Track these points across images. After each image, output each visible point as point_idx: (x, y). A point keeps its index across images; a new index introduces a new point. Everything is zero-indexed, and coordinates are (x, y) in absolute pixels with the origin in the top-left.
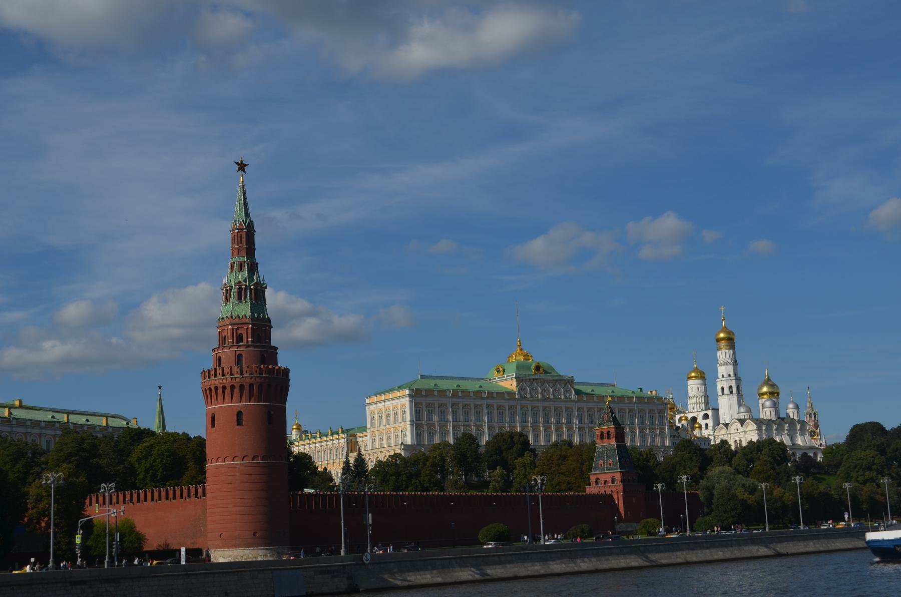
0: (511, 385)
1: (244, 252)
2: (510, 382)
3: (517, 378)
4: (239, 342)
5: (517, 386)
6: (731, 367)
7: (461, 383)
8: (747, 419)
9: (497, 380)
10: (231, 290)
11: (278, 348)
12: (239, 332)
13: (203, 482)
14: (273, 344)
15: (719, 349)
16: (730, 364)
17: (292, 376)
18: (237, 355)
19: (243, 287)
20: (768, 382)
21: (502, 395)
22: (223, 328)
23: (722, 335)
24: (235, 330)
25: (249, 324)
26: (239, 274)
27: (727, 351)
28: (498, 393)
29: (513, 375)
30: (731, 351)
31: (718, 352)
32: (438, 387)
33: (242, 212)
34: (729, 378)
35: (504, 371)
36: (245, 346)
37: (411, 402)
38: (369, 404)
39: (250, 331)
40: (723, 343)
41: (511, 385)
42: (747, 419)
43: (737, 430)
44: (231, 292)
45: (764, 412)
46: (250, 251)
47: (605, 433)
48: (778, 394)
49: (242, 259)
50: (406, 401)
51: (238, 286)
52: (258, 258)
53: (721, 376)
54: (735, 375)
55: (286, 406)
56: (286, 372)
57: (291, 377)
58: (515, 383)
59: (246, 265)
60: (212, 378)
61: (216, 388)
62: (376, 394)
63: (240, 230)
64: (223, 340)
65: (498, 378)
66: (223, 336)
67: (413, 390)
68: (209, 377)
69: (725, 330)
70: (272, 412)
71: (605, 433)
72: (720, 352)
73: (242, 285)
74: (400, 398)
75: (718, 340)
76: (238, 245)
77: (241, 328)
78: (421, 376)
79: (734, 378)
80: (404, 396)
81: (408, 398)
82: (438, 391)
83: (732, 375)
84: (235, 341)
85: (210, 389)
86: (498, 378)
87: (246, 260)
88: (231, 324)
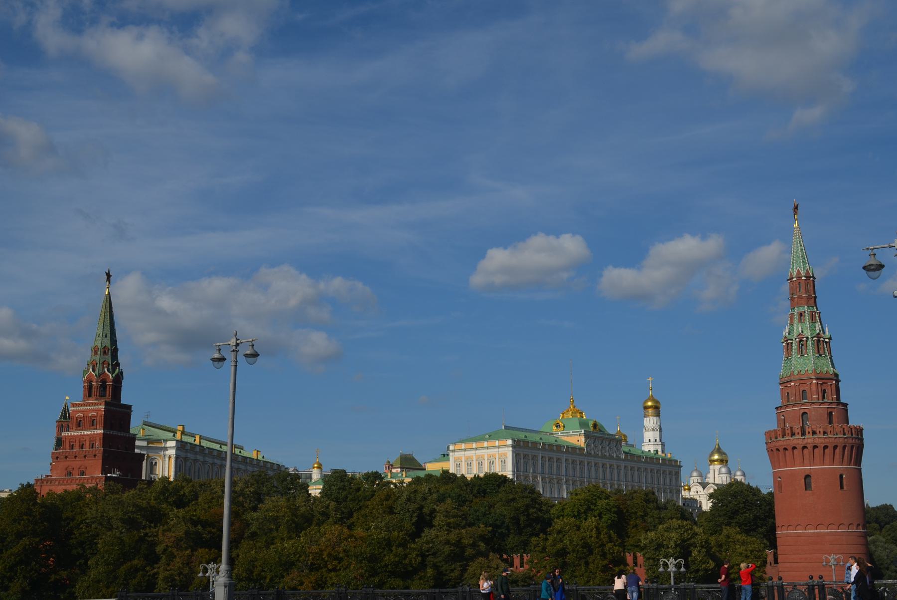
0: (578, 441)
2: (578, 438)
3: (585, 434)
4: (803, 399)
5: (585, 443)
6: (658, 433)
7: (527, 434)
8: (710, 483)
12: (824, 388)
15: (645, 416)
16: (657, 430)
20: (719, 451)
21: (573, 450)
23: (650, 404)
24: (819, 385)
25: (833, 379)
27: (655, 418)
28: (572, 448)
29: (581, 431)
30: (658, 418)
32: (557, 443)
34: (656, 443)
35: (564, 427)
36: (836, 404)
37: (513, 452)
38: (454, 451)
40: (650, 411)
41: (578, 441)
42: (710, 483)
43: (697, 492)
48: (727, 461)
50: (509, 452)
51: (798, 338)
53: (648, 441)
54: (660, 441)
58: (583, 439)
62: (462, 441)
65: (561, 433)
67: (515, 441)
69: (652, 399)
72: (648, 418)
73: (821, 337)
74: (499, 448)
75: (646, 408)
77: (825, 383)
78: (505, 426)
79: (660, 443)
80: (506, 446)
81: (510, 449)
82: (556, 446)
83: (658, 440)
86: (561, 433)
87: (806, 309)
88: (817, 379)
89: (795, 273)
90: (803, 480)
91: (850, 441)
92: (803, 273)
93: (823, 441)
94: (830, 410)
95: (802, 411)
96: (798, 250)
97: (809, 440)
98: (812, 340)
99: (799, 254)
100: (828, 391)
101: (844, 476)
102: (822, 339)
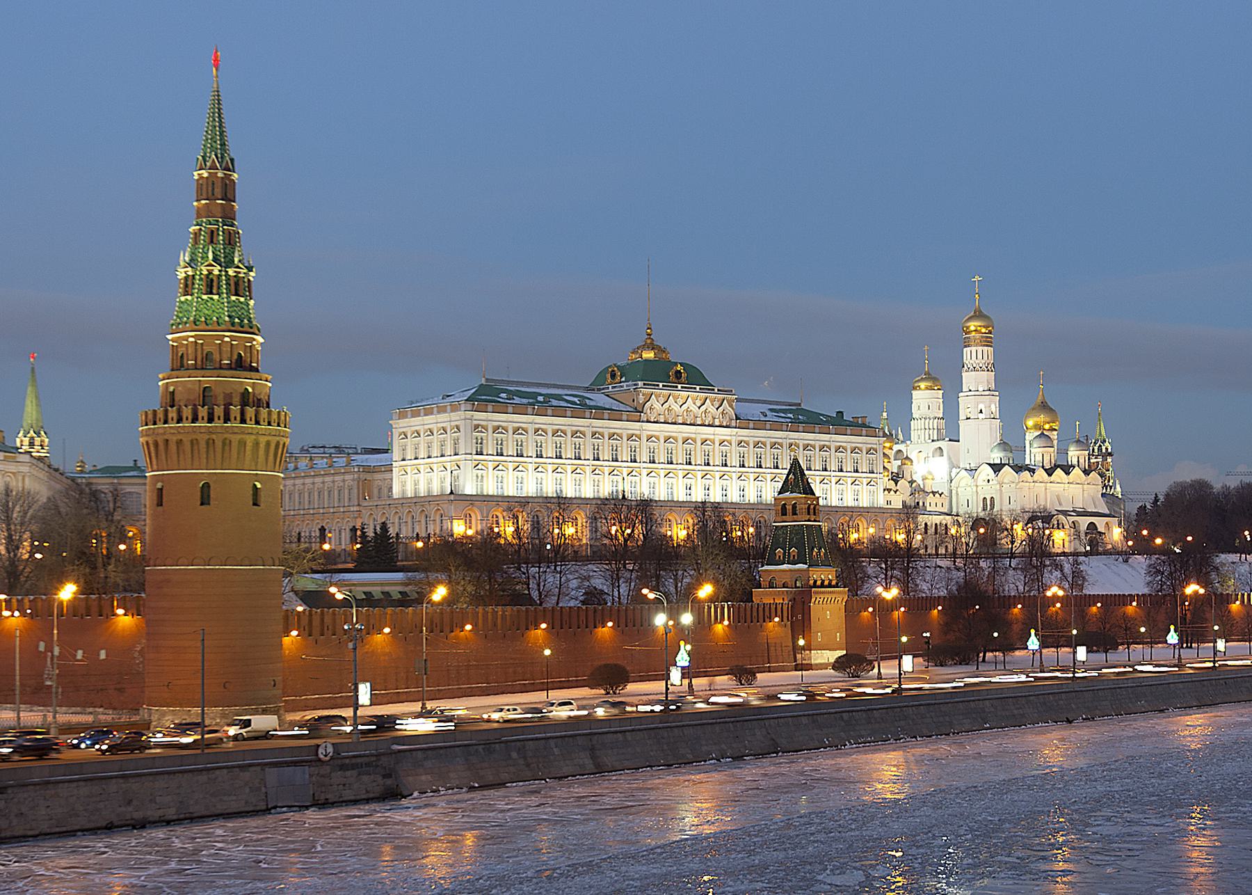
8: (1005, 465)
9: (610, 389)
26: (208, 250)
27: (980, 349)
31: (965, 349)
33: (215, 142)
43: (988, 481)
45: (1032, 455)
47: (789, 508)
59: (221, 233)
66: (180, 354)
70: (259, 485)
71: (789, 508)
72: (969, 349)
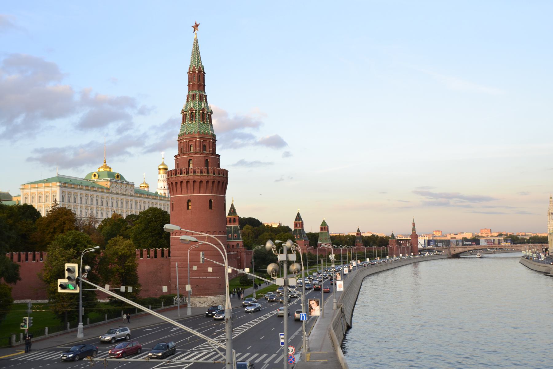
1: (196, 87)
10: (186, 114)
11: (220, 156)
12: (190, 144)
13: (168, 246)
14: (217, 153)
17: (229, 173)
18: (188, 160)
19: (194, 111)
22: (181, 141)
39: (198, 144)
44: (186, 116)
46: (201, 86)
49: (194, 92)
52: (208, 90)
55: (226, 196)
56: (225, 172)
57: (229, 176)
60: (174, 176)
61: (176, 183)
63: (194, 72)
64: (181, 149)
68: (172, 176)
73: (193, 111)
76: (192, 83)
84: (187, 150)
85: (172, 183)
87: (197, 92)
89: (192, 68)
90: (186, 203)
91: (218, 178)
92: (197, 69)
93: (200, 178)
94: (206, 158)
95: (188, 159)
96: (195, 53)
97: (191, 177)
98: (199, 112)
99: (196, 56)
100: (207, 146)
101: (212, 201)
102: (205, 112)
